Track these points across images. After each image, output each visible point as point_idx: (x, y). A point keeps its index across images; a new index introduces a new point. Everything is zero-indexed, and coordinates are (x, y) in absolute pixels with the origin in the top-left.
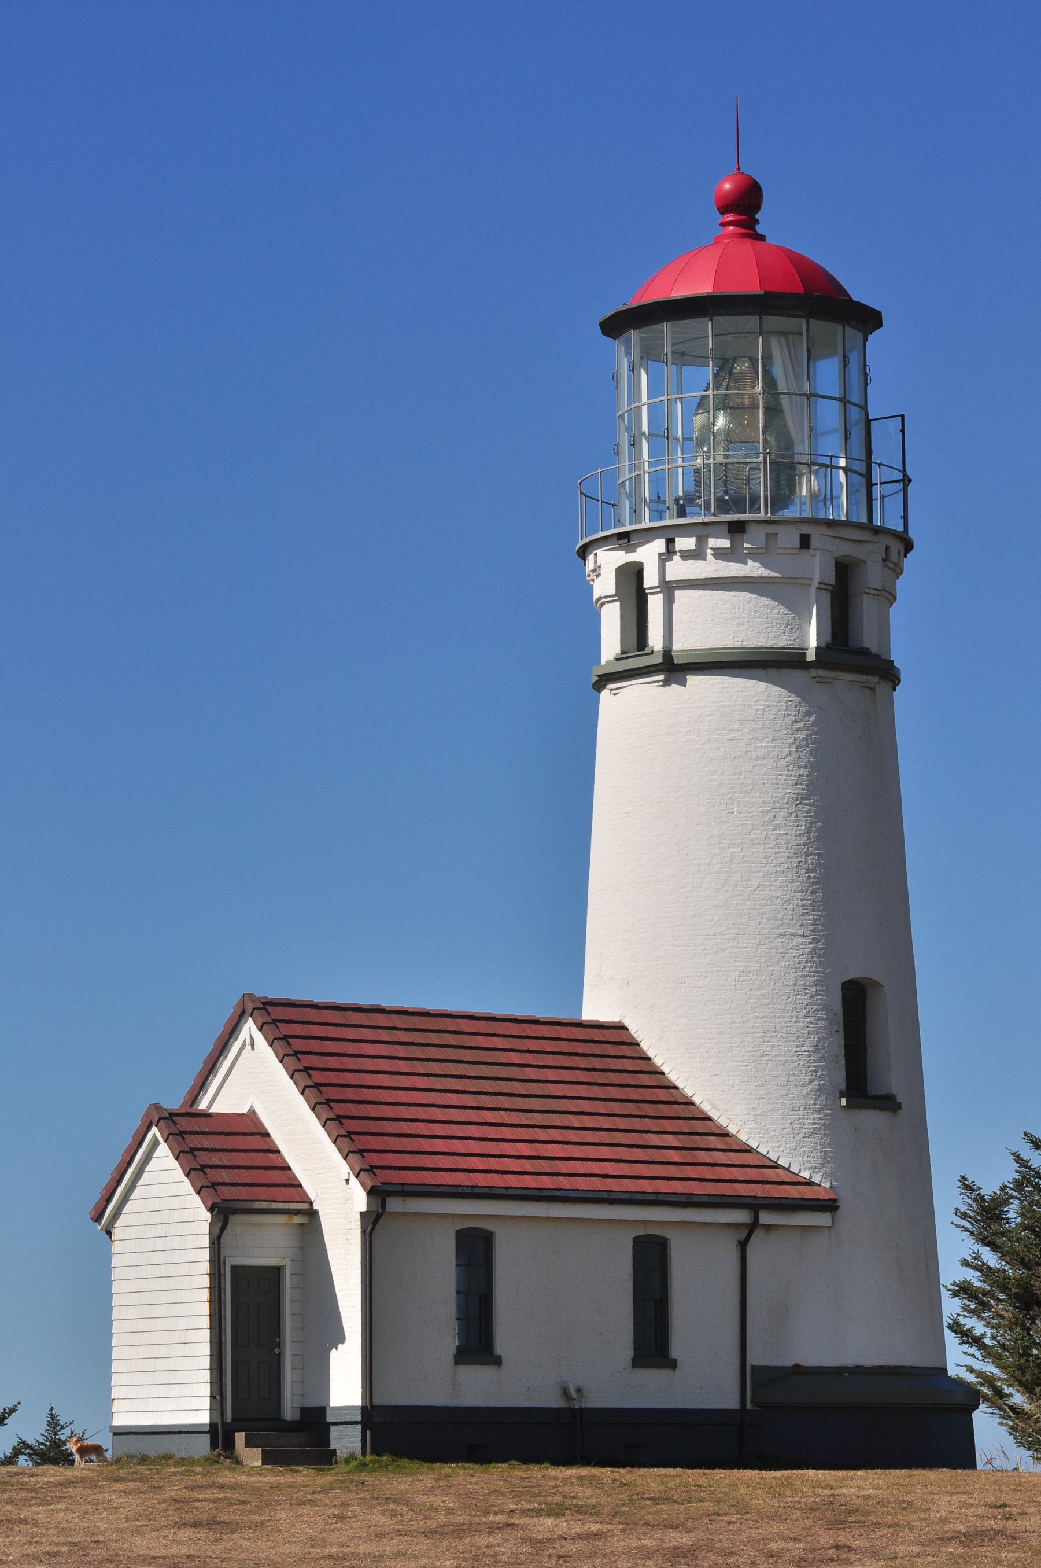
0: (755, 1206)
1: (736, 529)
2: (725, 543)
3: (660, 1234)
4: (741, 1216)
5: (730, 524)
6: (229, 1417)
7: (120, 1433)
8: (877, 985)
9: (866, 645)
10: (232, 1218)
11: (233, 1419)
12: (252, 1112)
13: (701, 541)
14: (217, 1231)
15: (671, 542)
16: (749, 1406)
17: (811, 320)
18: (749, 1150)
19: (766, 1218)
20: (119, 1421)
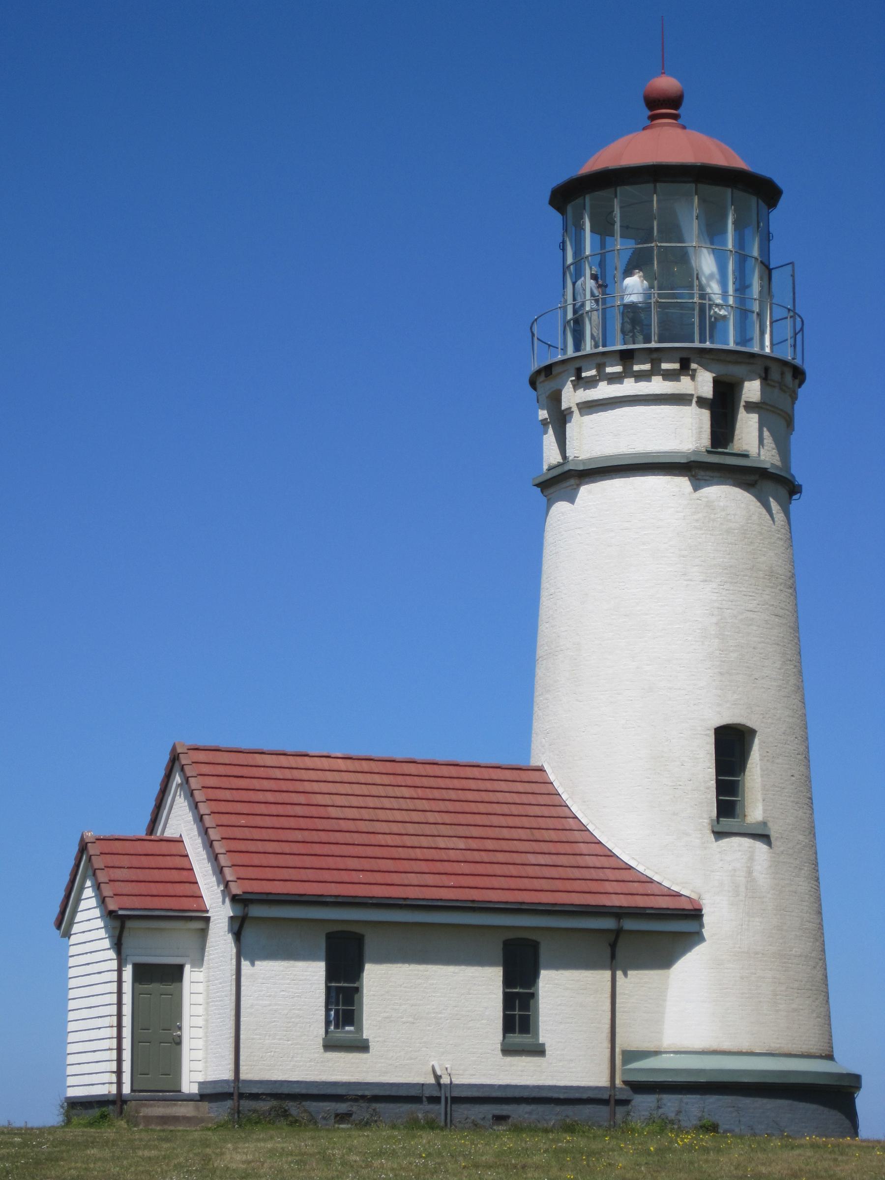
0: (619, 913)
1: (627, 357)
2: (618, 369)
3: (534, 938)
4: (608, 924)
5: (621, 351)
6: (126, 1089)
7: (76, 1105)
8: (752, 732)
9: (745, 447)
10: (129, 924)
11: (132, 1090)
12: (180, 841)
13: (600, 367)
14: (117, 933)
15: (579, 371)
16: (618, 1082)
17: (699, 185)
18: (630, 868)
19: (629, 925)
20: (72, 1093)
